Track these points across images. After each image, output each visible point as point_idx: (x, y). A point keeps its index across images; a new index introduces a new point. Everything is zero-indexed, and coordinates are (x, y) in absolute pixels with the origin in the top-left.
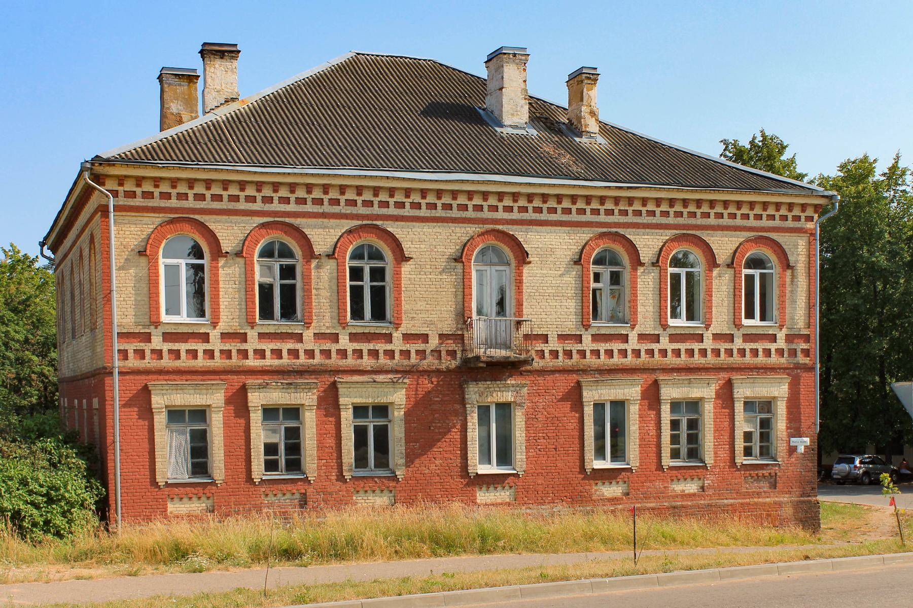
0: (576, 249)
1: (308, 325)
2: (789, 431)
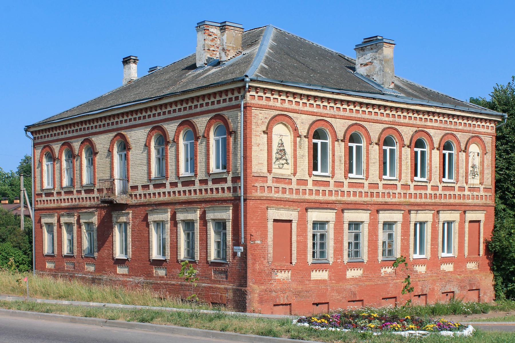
2: (233, 241)
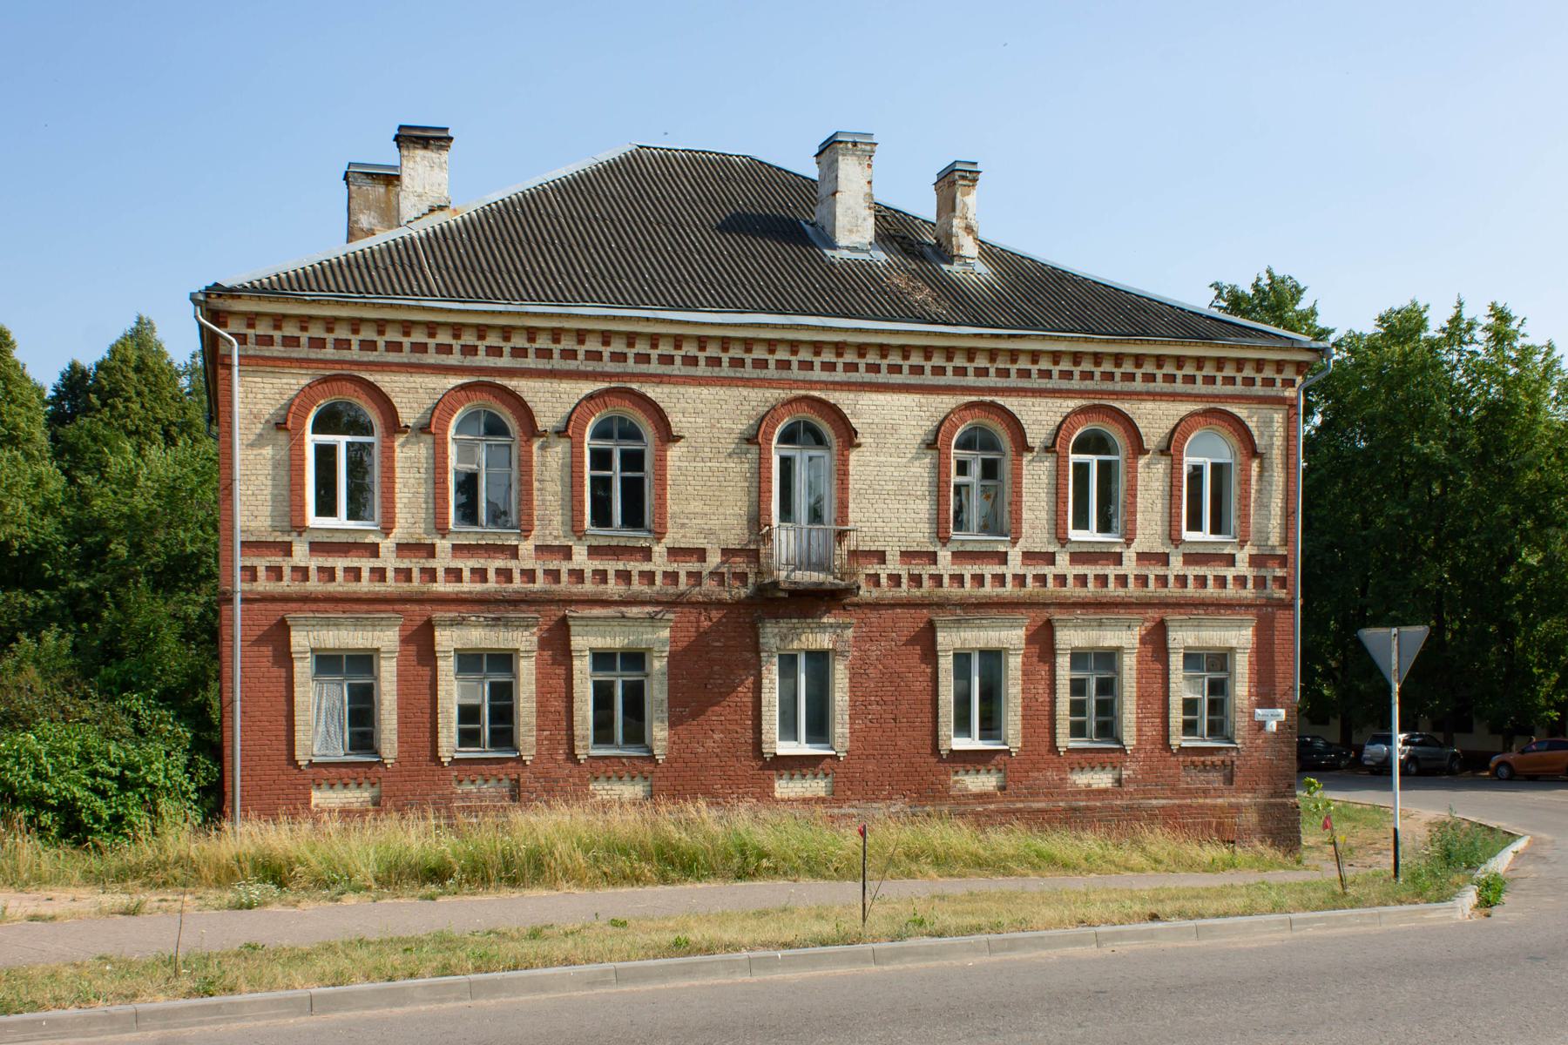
0: (929, 425)
1: (526, 534)
